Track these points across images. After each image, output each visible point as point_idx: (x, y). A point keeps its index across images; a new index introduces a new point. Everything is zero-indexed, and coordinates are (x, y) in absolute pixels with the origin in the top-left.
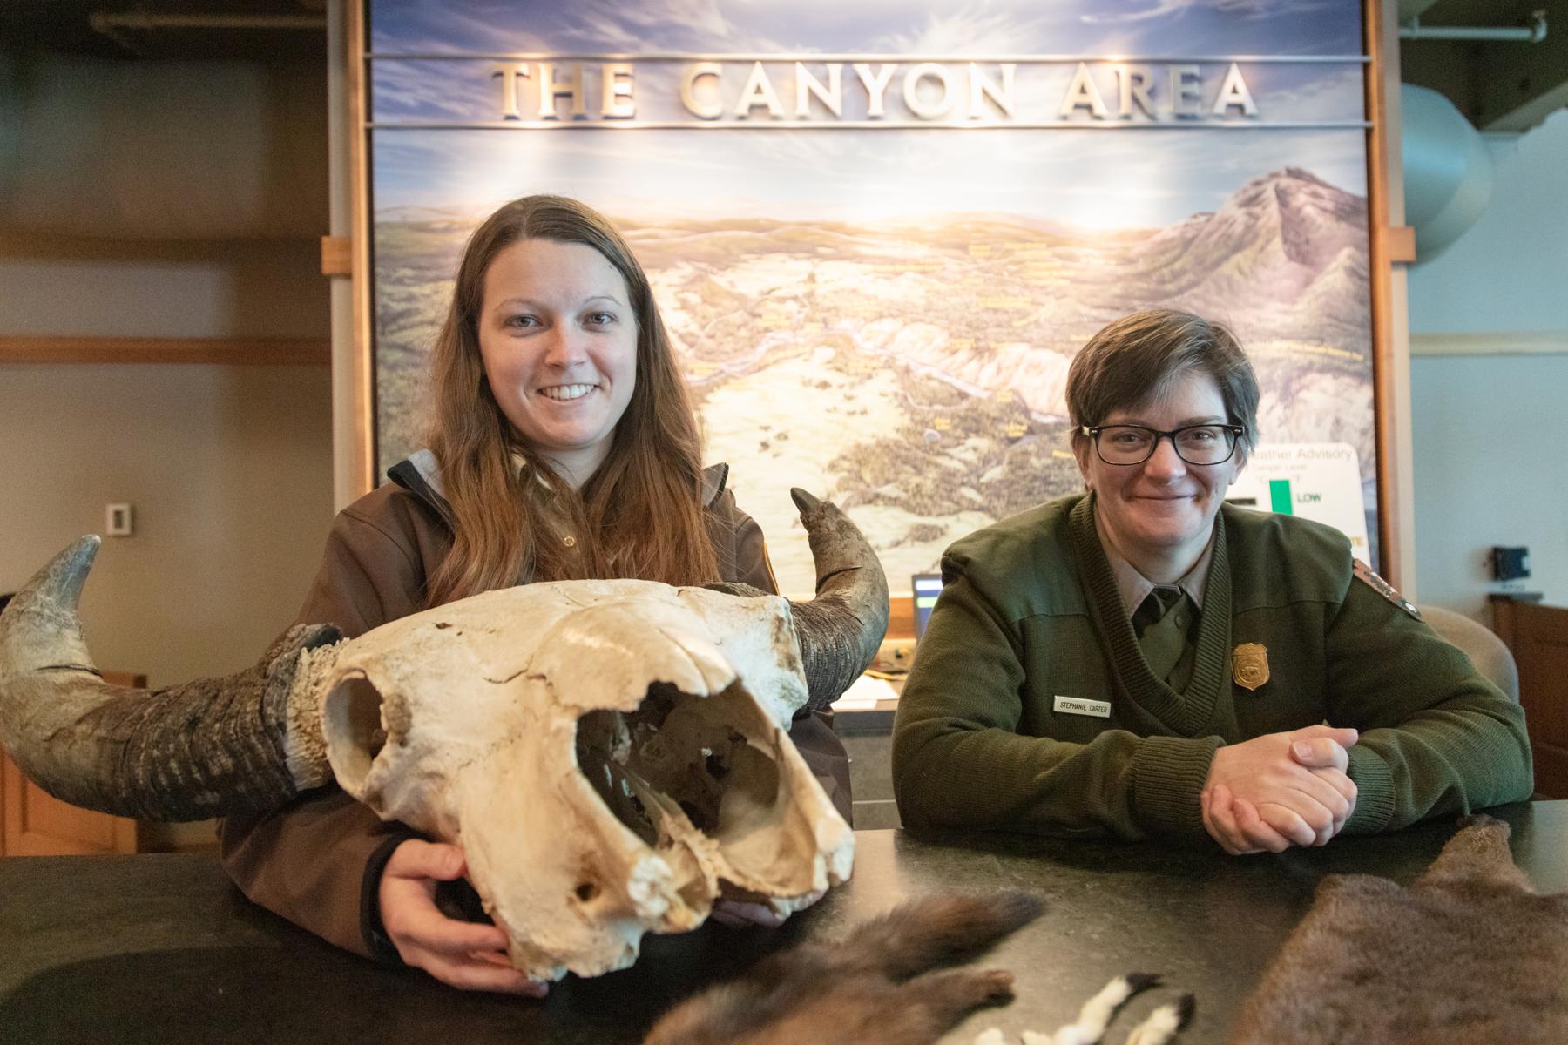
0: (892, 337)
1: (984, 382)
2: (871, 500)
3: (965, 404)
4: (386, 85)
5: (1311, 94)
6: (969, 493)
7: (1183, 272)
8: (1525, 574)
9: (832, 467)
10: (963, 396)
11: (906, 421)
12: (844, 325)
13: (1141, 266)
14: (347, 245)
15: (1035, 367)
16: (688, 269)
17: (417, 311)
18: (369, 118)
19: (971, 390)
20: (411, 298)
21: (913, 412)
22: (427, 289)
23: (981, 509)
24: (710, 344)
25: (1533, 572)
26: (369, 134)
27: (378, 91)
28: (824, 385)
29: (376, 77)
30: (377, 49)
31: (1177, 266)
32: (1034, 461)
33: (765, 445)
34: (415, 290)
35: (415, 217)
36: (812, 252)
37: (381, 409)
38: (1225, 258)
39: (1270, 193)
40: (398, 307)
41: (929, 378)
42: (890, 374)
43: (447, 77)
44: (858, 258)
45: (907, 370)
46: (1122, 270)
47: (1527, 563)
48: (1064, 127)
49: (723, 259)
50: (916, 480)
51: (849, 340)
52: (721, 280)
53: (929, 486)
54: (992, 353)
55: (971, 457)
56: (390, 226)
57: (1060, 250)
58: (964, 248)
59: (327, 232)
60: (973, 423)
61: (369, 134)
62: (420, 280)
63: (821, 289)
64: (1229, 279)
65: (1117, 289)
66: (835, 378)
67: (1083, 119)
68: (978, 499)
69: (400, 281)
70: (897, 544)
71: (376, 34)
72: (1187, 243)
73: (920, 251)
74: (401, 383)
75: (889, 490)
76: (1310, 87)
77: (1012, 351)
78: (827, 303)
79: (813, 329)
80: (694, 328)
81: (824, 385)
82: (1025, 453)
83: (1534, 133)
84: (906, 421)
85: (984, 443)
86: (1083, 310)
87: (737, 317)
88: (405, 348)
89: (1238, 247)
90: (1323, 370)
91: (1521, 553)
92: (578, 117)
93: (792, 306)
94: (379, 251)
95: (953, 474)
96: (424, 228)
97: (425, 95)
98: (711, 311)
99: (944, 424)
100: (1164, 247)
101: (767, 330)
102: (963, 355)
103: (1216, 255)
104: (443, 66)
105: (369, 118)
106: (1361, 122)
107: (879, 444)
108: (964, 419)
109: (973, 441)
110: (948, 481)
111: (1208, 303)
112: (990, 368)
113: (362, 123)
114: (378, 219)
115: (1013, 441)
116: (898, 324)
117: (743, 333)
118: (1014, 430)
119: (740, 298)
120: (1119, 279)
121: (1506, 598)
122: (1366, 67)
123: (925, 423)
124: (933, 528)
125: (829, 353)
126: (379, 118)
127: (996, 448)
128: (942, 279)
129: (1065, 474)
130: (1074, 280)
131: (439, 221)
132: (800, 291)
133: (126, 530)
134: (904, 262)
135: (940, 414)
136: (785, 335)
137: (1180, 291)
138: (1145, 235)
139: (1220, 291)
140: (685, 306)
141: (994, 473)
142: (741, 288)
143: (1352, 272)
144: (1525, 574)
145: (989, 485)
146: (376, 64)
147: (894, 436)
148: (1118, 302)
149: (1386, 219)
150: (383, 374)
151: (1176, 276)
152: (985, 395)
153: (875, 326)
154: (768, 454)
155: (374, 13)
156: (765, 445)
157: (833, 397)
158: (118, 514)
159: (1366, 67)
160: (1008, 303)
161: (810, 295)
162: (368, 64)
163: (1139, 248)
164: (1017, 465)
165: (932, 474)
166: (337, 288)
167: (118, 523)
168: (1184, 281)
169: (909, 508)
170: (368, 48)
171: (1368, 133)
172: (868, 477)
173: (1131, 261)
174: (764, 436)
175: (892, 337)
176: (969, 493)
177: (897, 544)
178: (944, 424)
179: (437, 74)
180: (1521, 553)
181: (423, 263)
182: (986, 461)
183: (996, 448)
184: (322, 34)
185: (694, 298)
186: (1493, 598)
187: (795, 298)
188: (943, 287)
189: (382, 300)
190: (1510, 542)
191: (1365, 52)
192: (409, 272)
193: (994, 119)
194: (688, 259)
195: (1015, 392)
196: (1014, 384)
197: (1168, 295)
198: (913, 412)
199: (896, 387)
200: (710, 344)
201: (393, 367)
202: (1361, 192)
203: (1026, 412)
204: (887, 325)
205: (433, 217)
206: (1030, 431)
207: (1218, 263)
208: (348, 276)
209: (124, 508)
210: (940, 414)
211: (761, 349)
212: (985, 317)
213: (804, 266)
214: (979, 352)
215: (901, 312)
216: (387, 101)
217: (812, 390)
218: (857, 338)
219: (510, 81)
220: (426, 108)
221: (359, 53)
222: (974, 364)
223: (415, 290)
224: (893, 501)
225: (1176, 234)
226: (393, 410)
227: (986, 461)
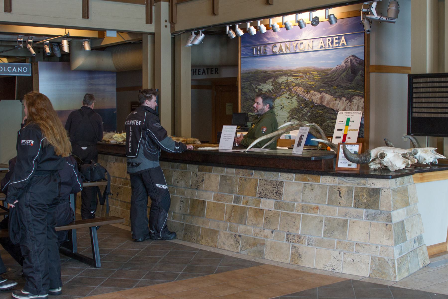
5: (356, 40)
7: (336, 76)
10: (305, 100)
12: (291, 88)
13: (330, 76)
15: (315, 95)
38: (342, 73)
39: (349, 60)
40: (243, 86)
42: (296, 96)
44: (293, 76)
46: (327, 76)
54: (309, 92)
55: (306, 111)
62: (245, 82)
66: (290, 97)
73: (301, 74)
79: (287, 88)
87: (278, 87)
88: (244, 92)
89: (344, 71)
90: (356, 96)
102: (305, 93)
109: (306, 108)
112: (309, 95)
115: (312, 108)
118: (312, 106)
119: (279, 83)
132: (286, 82)
140: (273, 85)
141: (309, 114)
151: (335, 77)
161: (287, 82)
164: (312, 113)
173: (329, 75)
178: (303, 105)
194: (273, 77)
197: (334, 81)
204: (296, 88)
206: (314, 107)
213: (286, 78)
214: (308, 92)
215: (297, 85)
220: (246, 54)
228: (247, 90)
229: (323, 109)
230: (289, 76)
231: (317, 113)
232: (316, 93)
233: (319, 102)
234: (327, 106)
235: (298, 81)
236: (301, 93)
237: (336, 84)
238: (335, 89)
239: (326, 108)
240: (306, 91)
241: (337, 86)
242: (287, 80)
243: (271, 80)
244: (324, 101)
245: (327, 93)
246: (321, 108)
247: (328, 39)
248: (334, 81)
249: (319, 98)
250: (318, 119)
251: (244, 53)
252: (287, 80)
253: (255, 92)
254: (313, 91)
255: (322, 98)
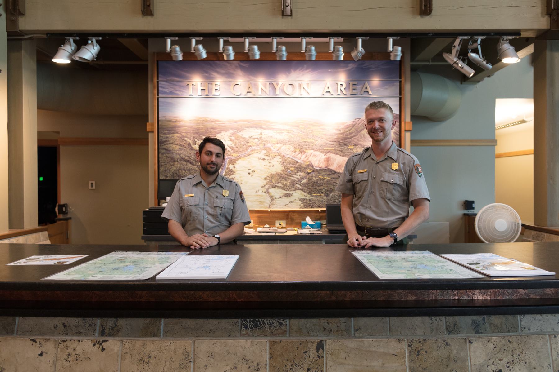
0: (280, 148)
1: (302, 159)
2: (274, 187)
3: (297, 164)
4: (161, 87)
5: (386, 89)
6: (298, 186)
7: (352, 133)
8: (473, 208)
9: (265, 179)
10: (297, 162)
11: (283, 168)
12: (269, 145)
13: (342, 131)
14: (153, 125)
15: (315, 156)
16: (232, 131)
17: (169, 141)
18: (158, 95)
19: (299, 161)
20: (167, 138)
21: (285, 166)
22: (171, 135)
23: (301, 190)
24: (237, 149)
25: (475, 208)
26: (158, 99)
27: (160, 89)
28: (264, 159)
29: (160, 85)
30: (160, 79)
31: (351, 131)
32: (314, 178)
33: (249, 173)
34: (168, 136)
35: (168, 118)
36: (262, 128)
37: (160, 163)
40: (164, 140)
41: (289, 158)
42: (280, 157)
43: (176, 85)
44: (273, 129)
45: (284, 156)
47: (474, 205)
48: (323, 96)
49: (240, 129)
50: (285, 182)
51: (270, 149)
52: (240, 134)
53: (288, 184)
54: (304, 152)
55: (299, 177)
56: (162, 120)
57: (321, 127)
58: (298, 127)
59: (148, 122)
60: (300, 169)
61: (158, 99)
62: (169, 133)
63: (263, 136)
64: (364, 135)
65: (336, 137)
66: (266, 158)
67: (328, 95)
68: (300, 187)
69: (165, 134)
70: (281, 197)
71: (160, 75)
72: (353, 126)
74: (165, 158)
75: (279, 185)
76: (386, 87)
77: (309, 152)
78: (265, 140)
79: (261, 146)
80: (233, 145)
81: (264, 159)
82: (312, 176)
83: (481, 83)
84: (283, 168)
85: (302, 174)
86: (327, 142)
87: (243, 143)
88: (166, 149)
91: (473, 202)
92: (207, 95)
93: (256, 140)
94: (160, 126)
95: (294, 181)
96: (170, 121)
97: (171, 89)
98: (237, 141)
99: (292, 169)
100: (348, 127)
101: (250, 146)
102: (297, 153)
103: (360, 129)
104: (175, 83)
105: (158, 95)
106: (398, 95)
107: (276, 174)
108: (297, 168)
110: (293, 182)
111: (358, 140)
112: (304, 156)
113: (156, 97)
114: (160, 119)
115: (309, 173)
116: (282, 145)
117: (245, 147)
118: (309, 171)
119: (244, 138)
120: (336, 134)
121: (467, 215)
122: (400, 82)
123: (288, 169)
124: (289, 194)
125: (265, 152)
126: (160, 95)
127: (305, 175)
128: (293, 134)
129: (348, 177)
130: (325, 135)
131: (174, 119)
132: (259, 137)
133: (94, 188)
134: (284, 130)
135: (292, 167)
136: (255, 147)
137: (351, 138)
138: (343, 124)
139: (361, 137)
140: (231, 140)
141: (304, 181)
142: (244, 136)
143: (395, 133)
144: (473, 208)
145: (303, 184)
146: (160, 82)
147: (280, 172)
148: (336, 140)
149: (405, 119)
150: (160, 155)
151: (350, 134)
152: (302, 162)
153: (276, 145)
154: (250, 176)
155: (159, 71)
156: (249, 173)
157: (266, 162)
158: (92, 184)
159: (400, 82)
160: (309, 140)
161: (261, 138)
162: (158, 82)
163: (342, 127)
164: (310, 179)
165: (289, 181)
166: (150, 135)
167: (92, 186)
168: (352, 135)
169: (284, 189)
170: (158, 79)
171: (400, 99)
172: (274, 182)
174: (249, 171)
175: (280, 148)
176: (298, 186)
177: (281, 197)
178: (292, 169)
179: (174, 84)
180: (473, 202)
181: (170, 129)
182: (302, 178)
183: (305, 175)
184: (147, 65)
185: (233, 138)
186: (465, 214)
187: (257, 138)
188: (293, 136)
189: (160, 138)
190: (470, 199)
191: (400, 78)
192: (167, 132)
193: (307, 95)
194: (232, 129)
195: (309, 161)
196: (310, 159)
197: (348, 138)
198: (285, 166)
199: (281, 160)
200: (237, 149)
201: (163, 154)
202: (398, 113)
203: (312, 166)
204: (279, 145)
205: (172, 119)
206: (313, 171)
207: (361, 131)
208: (153, 132)
209: (94, 182)
210: (292, 167)
211: (249, 151)
212: (303, 143)
213: (259, 131)
214: (302, 152)
215: (283, 142)
216: (162, 91)
217: (261, 160)
218: (272, 148)
219: (190, 86)
221: (156, 80)
222: (300, 155)
223: (168, 136)
224: (280, 187)
225: (351, 123)
226: (163, 164)
227: (302, 178)
228: (174, 146)
229: (329, 175)
230: (265, 129)
231: (320, 179)
232: (318, 153)
233: (323, 165)
234: (338, 171)
235: (284, 137)
236: (288, 153)
237: (352, 143)
238: (351, 149)
239: (336, 173)
240: (298, 150)
241: (355, 145)
242: (261, 134)
243: (228, 133)
244: (332, 164)
245: (337, 154)
246: (327, 173)
247: (339, 83)
248: (348, 138)
249: (322, 160)
250: (322, 187)
251: (166, 90)
252: (261, 134)
253: (192, 149)
254: (312, 151)
255: (328, 160)
